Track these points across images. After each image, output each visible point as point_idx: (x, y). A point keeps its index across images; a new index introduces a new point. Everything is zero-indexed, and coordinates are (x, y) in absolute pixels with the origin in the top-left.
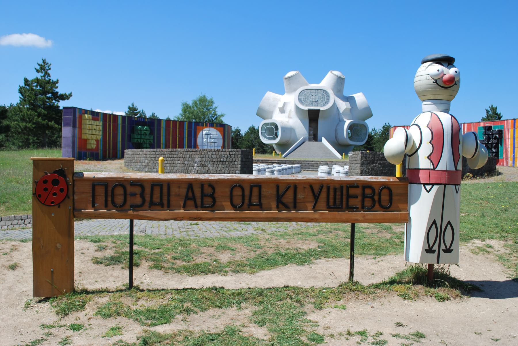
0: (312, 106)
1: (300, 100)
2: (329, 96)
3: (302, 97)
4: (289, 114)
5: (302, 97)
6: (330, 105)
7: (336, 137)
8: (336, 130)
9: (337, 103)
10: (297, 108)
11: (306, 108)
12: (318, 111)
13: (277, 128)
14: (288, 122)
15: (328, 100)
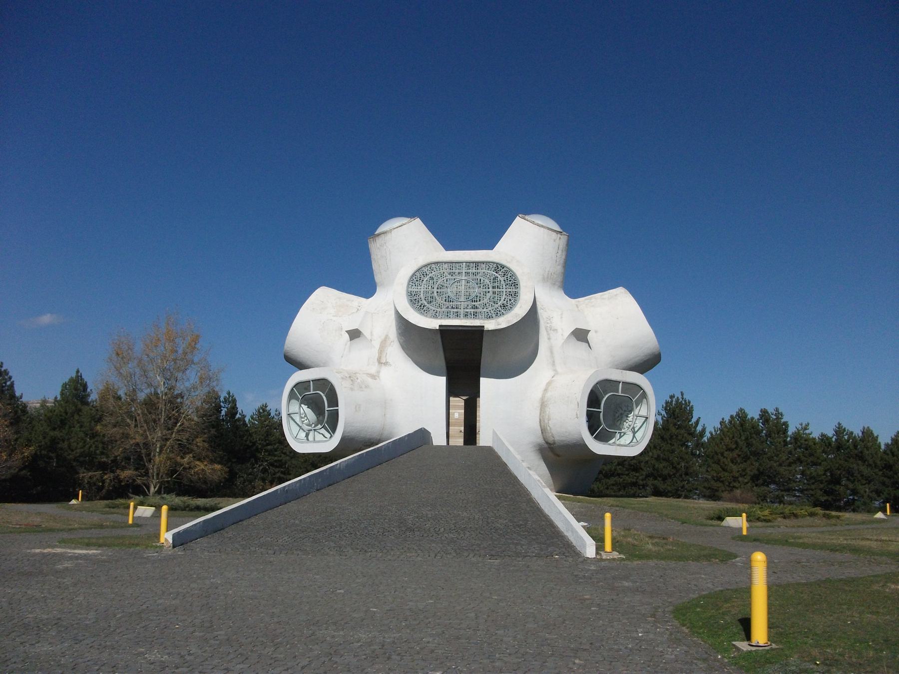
0: (457, 316)
1: (414, 300)
2: (516, 284)
3: (422, 289)
4: (381, 351)
5: (422, 289)
6: (519, 311)
7: (543, 431)
8: (543, 405)
9: (542, 315)
10: (406, 329)
11: (433, 324)
12: (480, 331)
13: (333, 399)
14: (374, 377)
15: (515, 295)
